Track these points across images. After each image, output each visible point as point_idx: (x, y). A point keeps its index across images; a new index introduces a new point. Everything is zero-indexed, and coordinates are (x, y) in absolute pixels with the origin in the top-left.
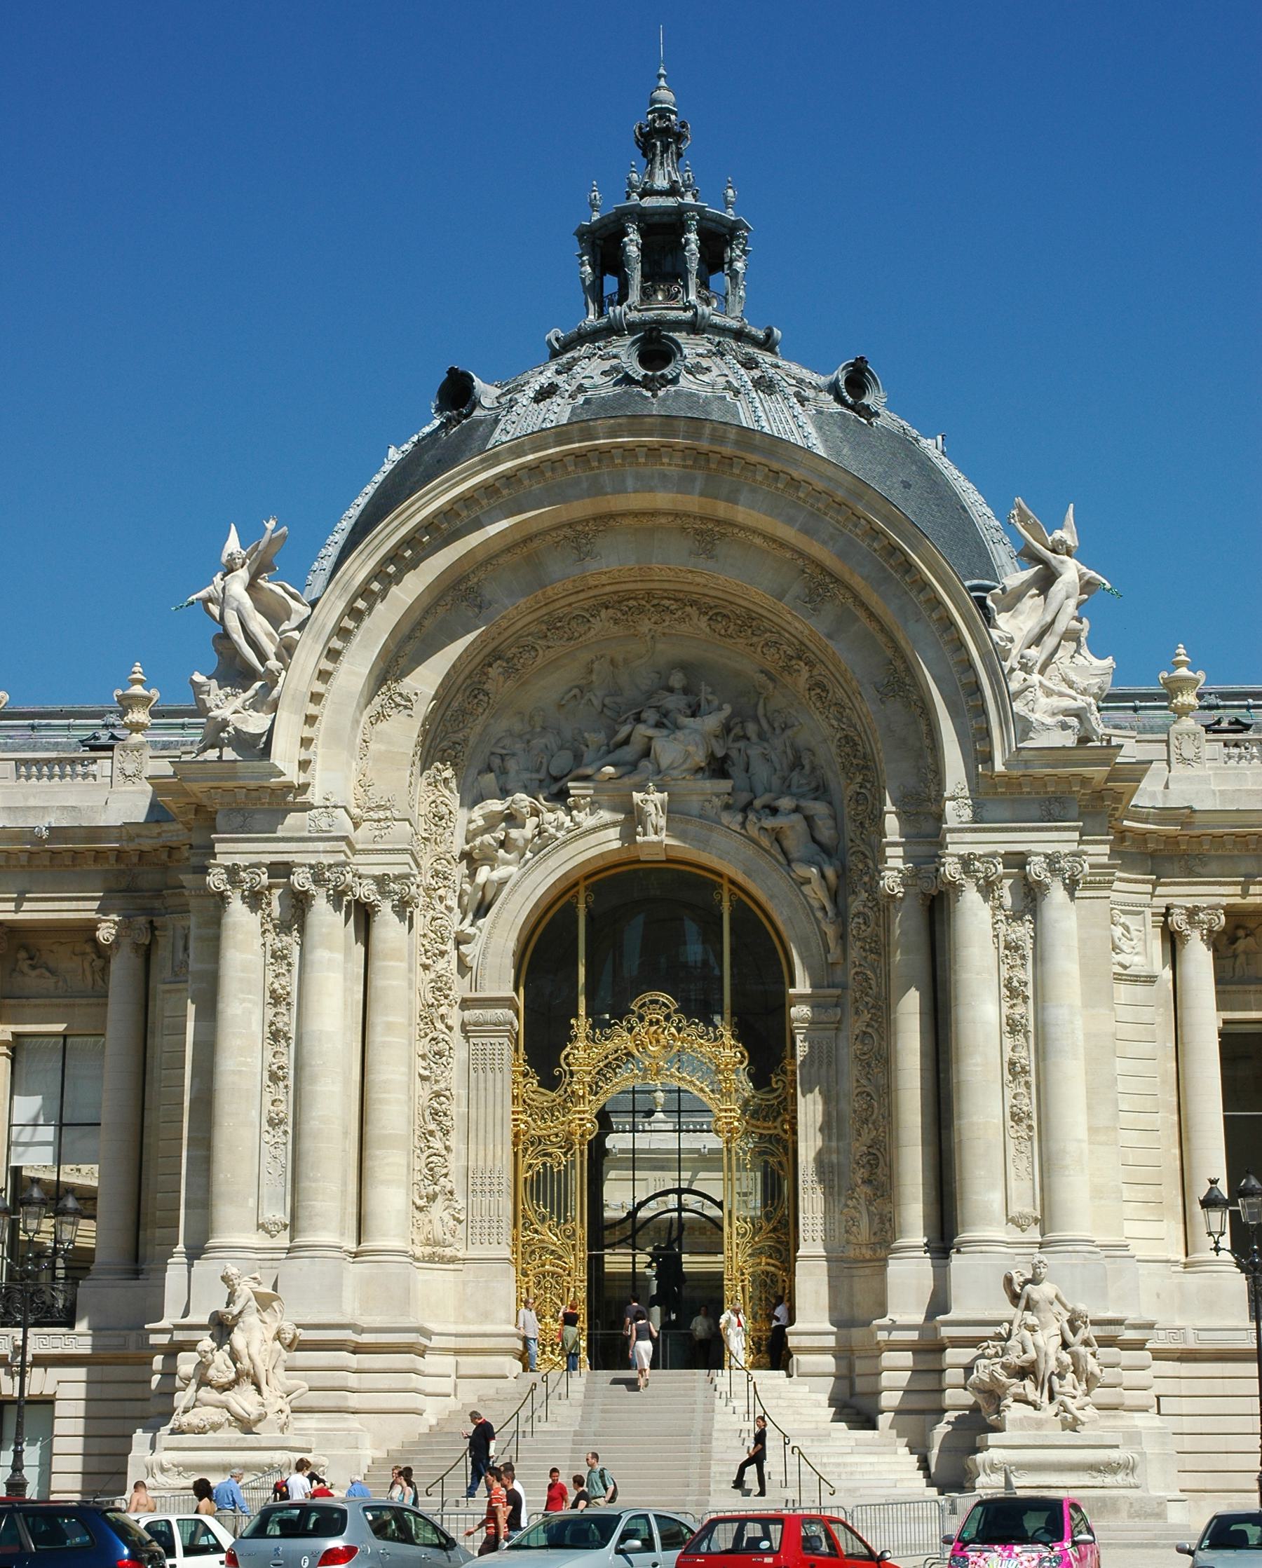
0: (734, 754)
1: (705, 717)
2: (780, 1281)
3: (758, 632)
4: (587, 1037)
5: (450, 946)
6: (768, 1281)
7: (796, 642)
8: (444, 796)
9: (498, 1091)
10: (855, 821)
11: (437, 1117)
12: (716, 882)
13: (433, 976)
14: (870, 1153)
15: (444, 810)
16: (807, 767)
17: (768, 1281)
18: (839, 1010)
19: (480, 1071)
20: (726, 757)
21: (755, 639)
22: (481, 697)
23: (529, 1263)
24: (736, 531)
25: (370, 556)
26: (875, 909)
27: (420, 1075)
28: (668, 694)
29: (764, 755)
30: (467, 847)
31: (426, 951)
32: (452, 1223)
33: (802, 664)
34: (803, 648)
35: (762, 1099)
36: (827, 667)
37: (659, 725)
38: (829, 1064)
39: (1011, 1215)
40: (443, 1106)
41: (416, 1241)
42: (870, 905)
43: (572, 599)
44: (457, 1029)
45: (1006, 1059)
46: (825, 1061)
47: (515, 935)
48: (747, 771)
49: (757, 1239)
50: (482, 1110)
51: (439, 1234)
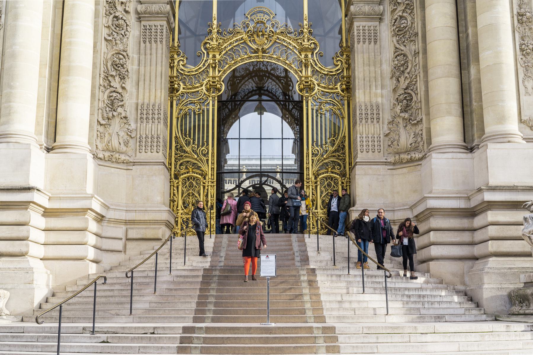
2: (340, 183)
4: (218, 32)
6: (333, 183)
9: (159, 55)
11: (117, 68)
17: (333, 183)
18: (381, 7)
19: (147, 42)
23: (179, 171)
27: (106, 40)
32: (126, 137)
38: (375, 43)
39: (523, 118)
40: (121, 61)
45: (515, 12)
46: (373, 40)
49: (325, 157)
50: (148, 68)
51: (115, 143)
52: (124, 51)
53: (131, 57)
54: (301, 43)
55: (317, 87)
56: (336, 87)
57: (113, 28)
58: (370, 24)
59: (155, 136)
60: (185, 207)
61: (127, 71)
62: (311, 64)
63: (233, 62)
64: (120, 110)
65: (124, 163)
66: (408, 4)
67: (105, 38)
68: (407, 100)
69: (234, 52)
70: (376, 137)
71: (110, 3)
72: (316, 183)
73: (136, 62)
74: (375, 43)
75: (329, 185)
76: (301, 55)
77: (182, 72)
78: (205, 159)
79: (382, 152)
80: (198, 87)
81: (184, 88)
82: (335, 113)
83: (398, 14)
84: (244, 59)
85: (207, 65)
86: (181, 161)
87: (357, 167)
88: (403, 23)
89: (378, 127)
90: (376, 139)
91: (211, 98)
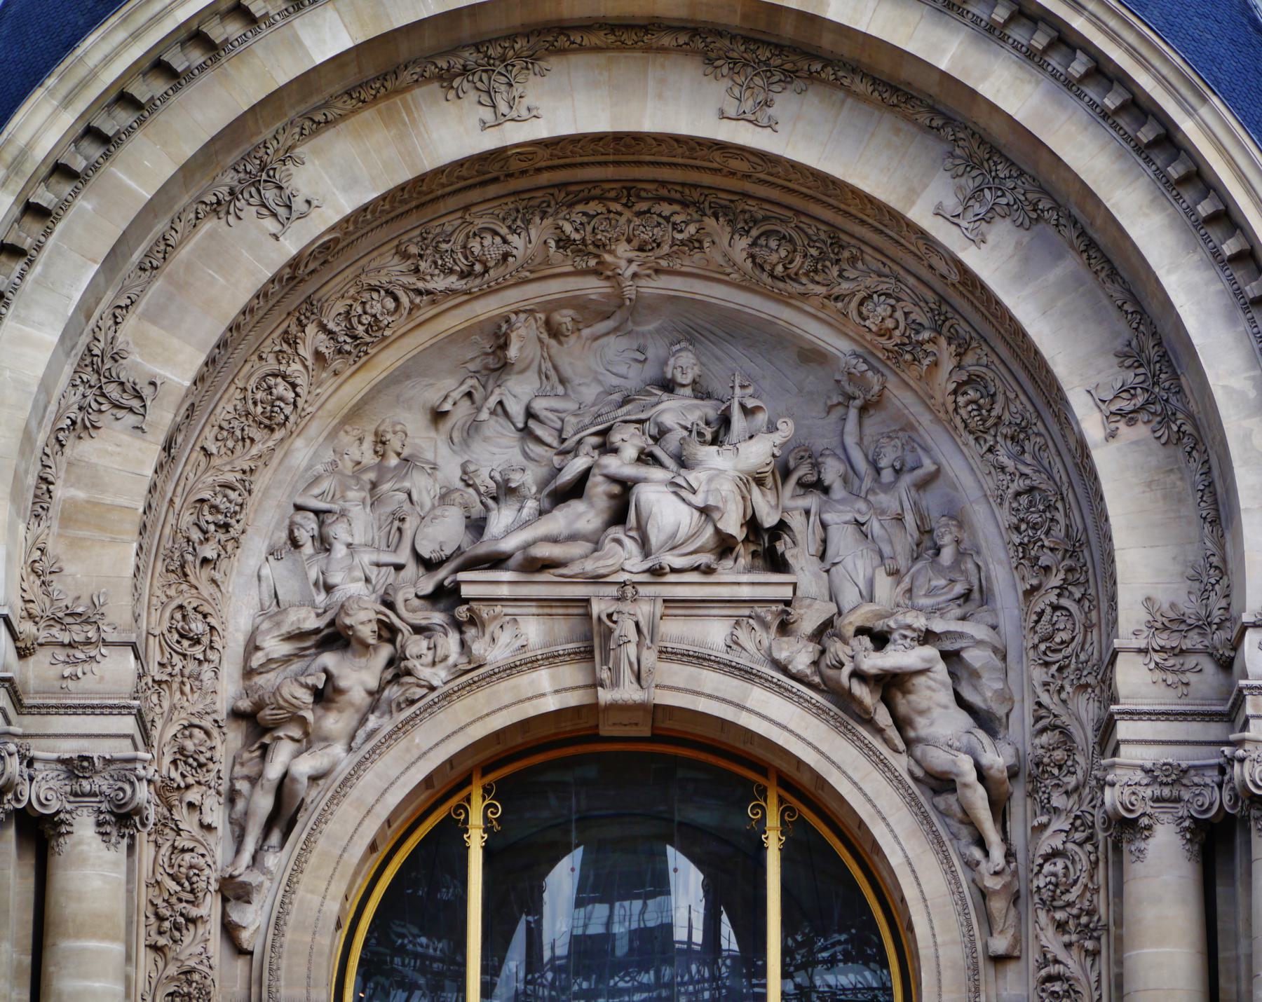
0: (796, 521)
1: (742, 447)
3: (851, 273)
5: (210, 907)
7: (930, 296)
10: (1047, 664)
12: (747, 783)
13: (172, 970)
15: (197, 626)
16: (947, 555)
20: (782, 527)
21: (845, 286)
22: (281, 389)
24: (817, 66)
25: (67, 102)
26: (1089, 847)
28: (665, 396)
30: (245, 705)
31: (160, 918)
33: (943, 341)
34: (944, 308)
36: (993, 349)
37: (646, 458)
42: (1079, 836)
43: (474, 196)
47: (339, 888)
48: (822, 557)
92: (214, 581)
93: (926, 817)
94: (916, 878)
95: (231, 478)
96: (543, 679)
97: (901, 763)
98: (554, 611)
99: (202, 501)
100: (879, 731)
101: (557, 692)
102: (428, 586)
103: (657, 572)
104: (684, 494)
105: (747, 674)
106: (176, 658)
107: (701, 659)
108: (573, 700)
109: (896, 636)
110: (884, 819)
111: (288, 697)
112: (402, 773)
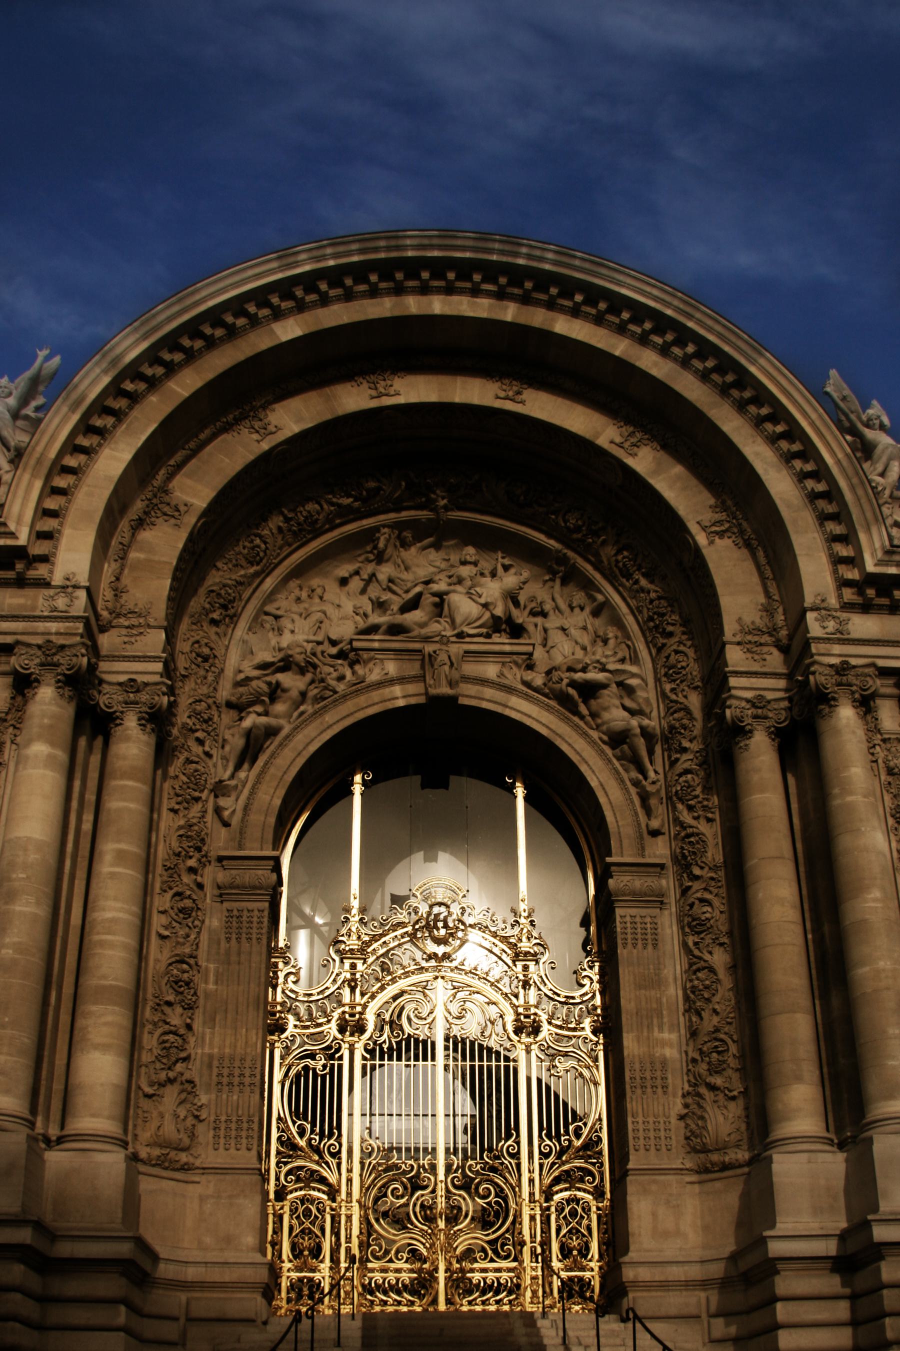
2: (594, 1209)
6: (580, 1210)
8: (208, 638)
11: (176, 987)
13: (182, 822)
14: (716, 1039)
17: (580, 1210)
18: (664, 882)
29: (564, 630)
31: (178, 795)
32: (190, 1121)
35: (566, 997)
38: (655, 946)
40: (186, 975)
41: (140, 1138)
44: (209, 890)
46: (650, 941)
49: (564, 1158)
51: (169, 1129)
52: (191, 956)
53: (203, 967)
54: (516, 945)
55: (545, 1027)
56: (581, 1026)
57: (173, 915)
58: (644, 912)
59: (245, 1119)
60: (295, 1257)
61: (195, 994)
62: (534, 982)
63: (389, 978)
64: (179, 1067)
65: (184, 1169)
66: (712, 879)
67: (158, 932)
68: (719, 1053)
69: (391, 960)
70: (662, 1122)
71: (170, 868)
72: (548, 1208)
73: (212, 978)
74: (655, 946)
75: (573, 1213)
76: (515, 965)
77: (293, 996)
78: (335, 1161)
79: (674, 1150)
80: (320, 1025)
81: (295, 1026)
82: (581, 1075)
83: (695, 896)
84: (408, 972)
85: (339, 982)
86: (289, 1166)
87: (629, 1178)
88: (704, 913)
89: (666, 1104)
90: (662, 1126)
91: (347, 1045)
92: (217, 633)
93: (610, 761)
94: (606, 792)
95: (230, 582)
96: (397, 690)
97: (595, 735)
98: (403, 657)
99: (212, 591)
100: (582, 718)
101: (404, 697)
102: (334, 651)
103: (461, 635)
104: (473, 597)
105: (509, 690)
106: (193, 666)
107: (483, 682)
108: (413, 701)
109: (590, 668)
110: (586, 762)
111: (255, 687)
112: (319, 735)
